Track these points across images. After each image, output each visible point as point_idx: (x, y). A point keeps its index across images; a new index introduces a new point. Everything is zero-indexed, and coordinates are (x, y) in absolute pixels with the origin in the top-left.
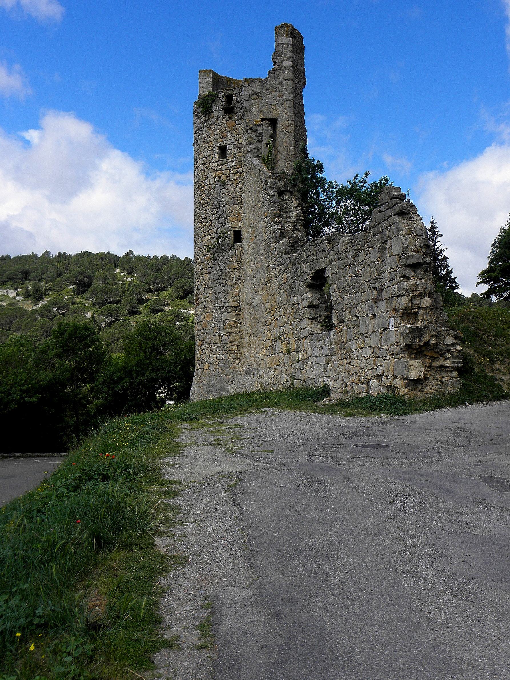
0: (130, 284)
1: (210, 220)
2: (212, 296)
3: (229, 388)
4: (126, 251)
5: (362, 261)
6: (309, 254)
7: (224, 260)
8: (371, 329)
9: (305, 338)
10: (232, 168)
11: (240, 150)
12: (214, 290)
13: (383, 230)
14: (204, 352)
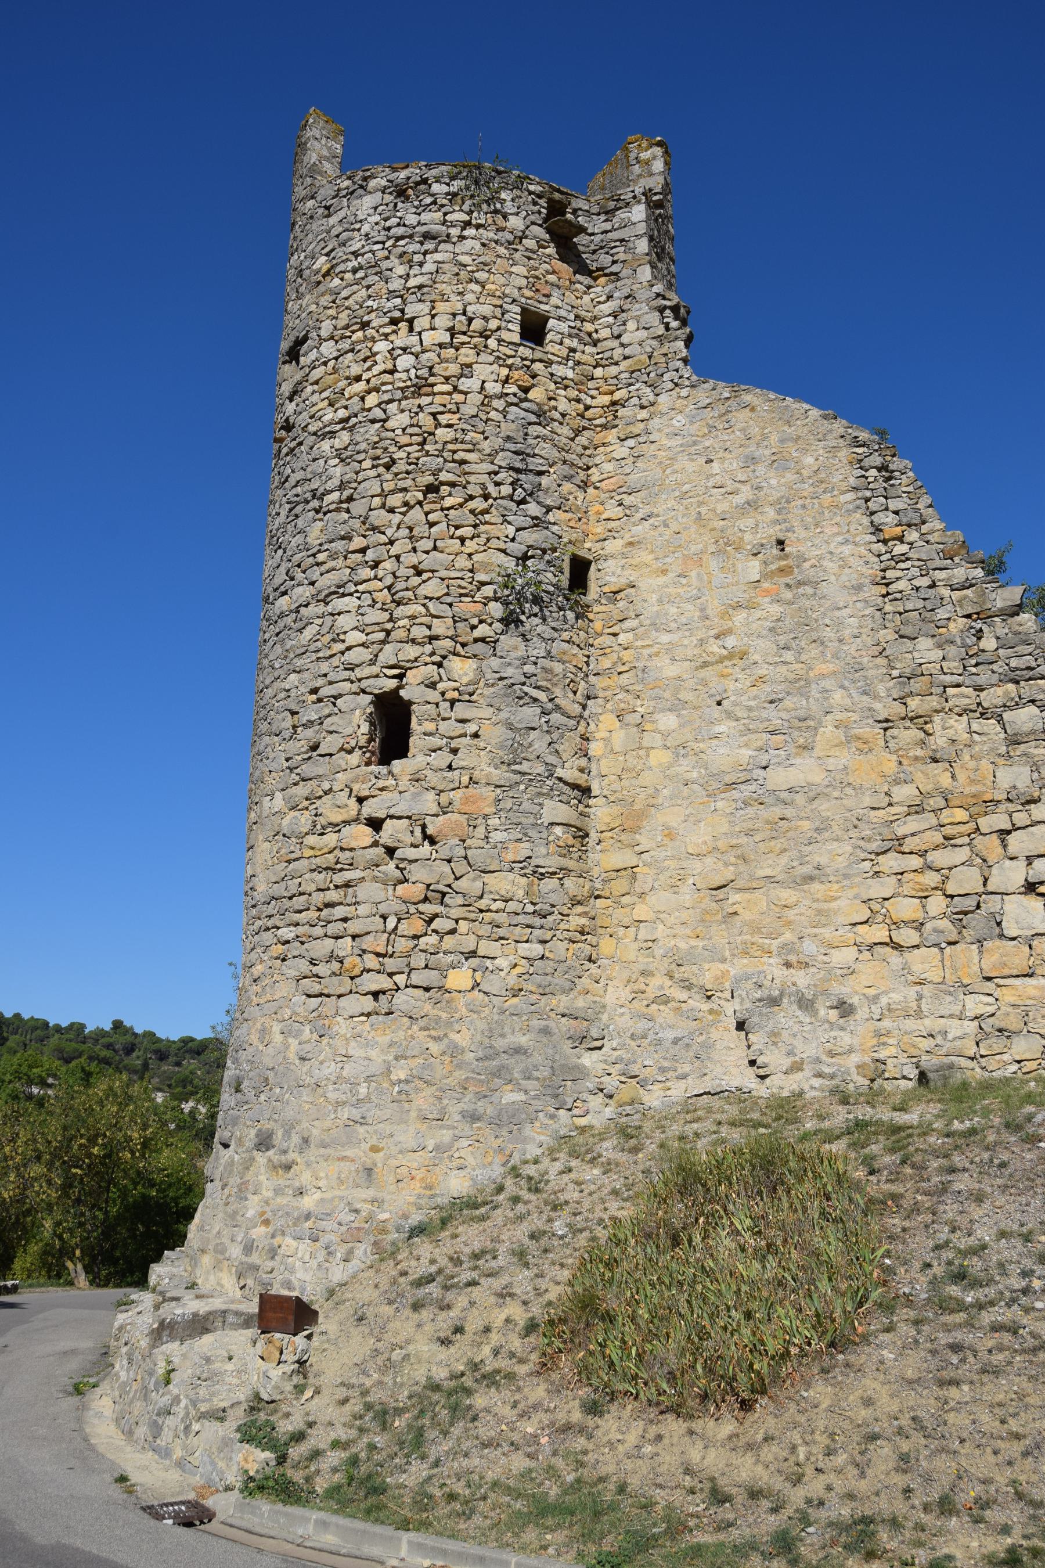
1: (486, 497)
2: (494, 734)
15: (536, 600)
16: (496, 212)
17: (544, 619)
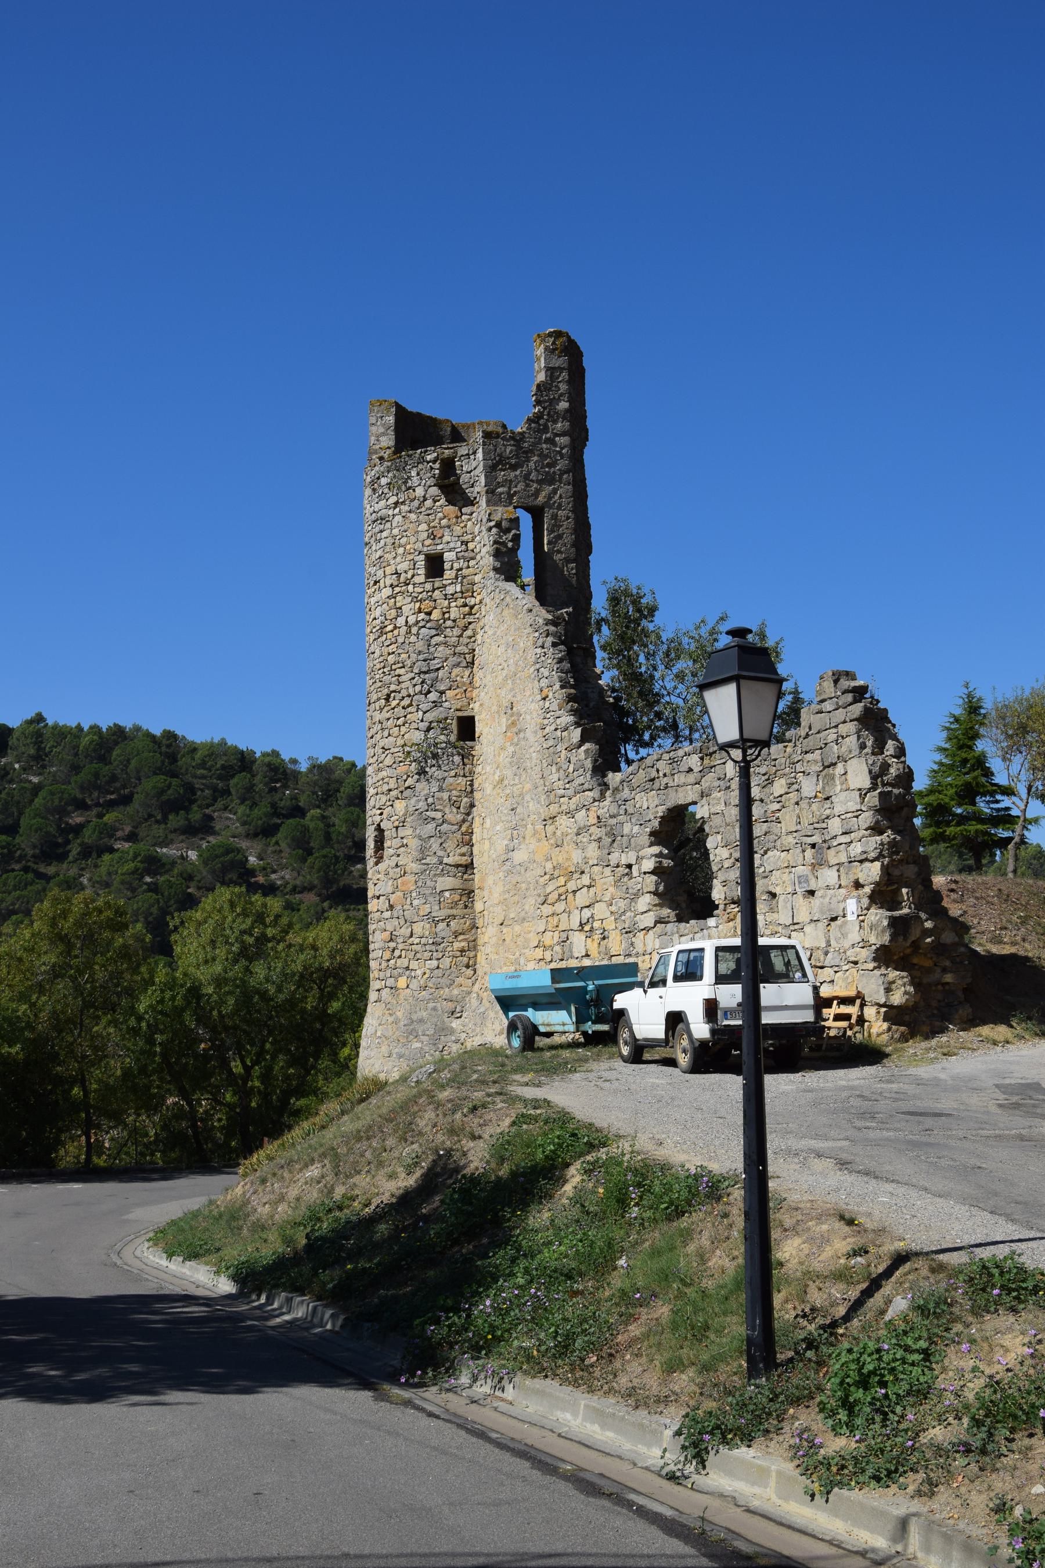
0: (37, 789)
1: (409, 696)
2: (414, 843)
3: (454, 1025)
4: (30, 715)
5: (781, 796)
6: (654, 774)
7: (439, 774)
8: (802, 917)
9: (647, 929)
10: (453, 597)
11: (472, 563)
12: (418, 831)
13: (826, 744)
14: (397, 953)
15: (435, 756)
16: (410, 488)
17: (439, 766)
